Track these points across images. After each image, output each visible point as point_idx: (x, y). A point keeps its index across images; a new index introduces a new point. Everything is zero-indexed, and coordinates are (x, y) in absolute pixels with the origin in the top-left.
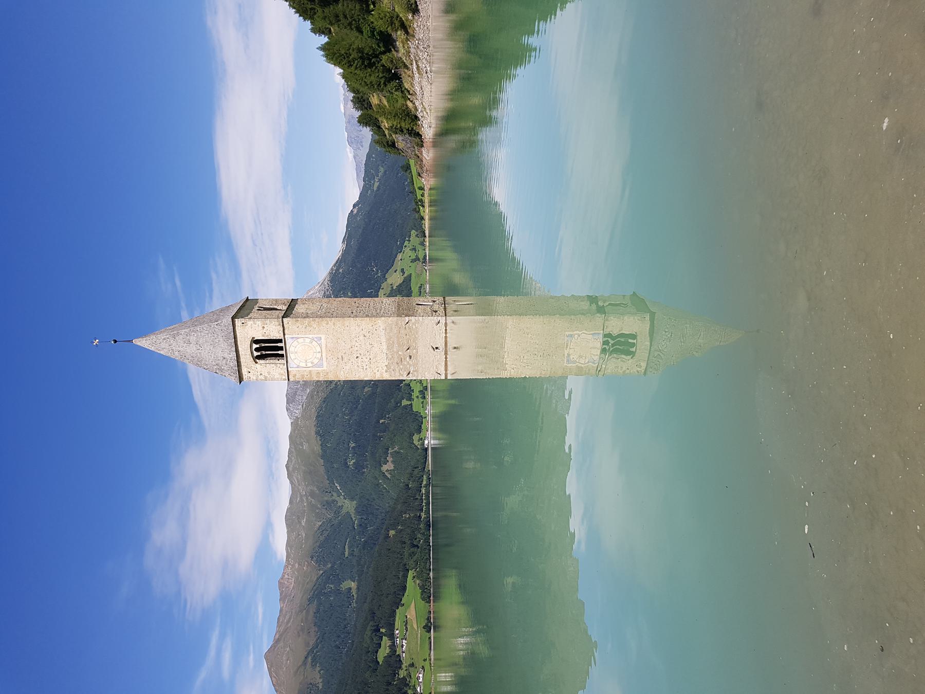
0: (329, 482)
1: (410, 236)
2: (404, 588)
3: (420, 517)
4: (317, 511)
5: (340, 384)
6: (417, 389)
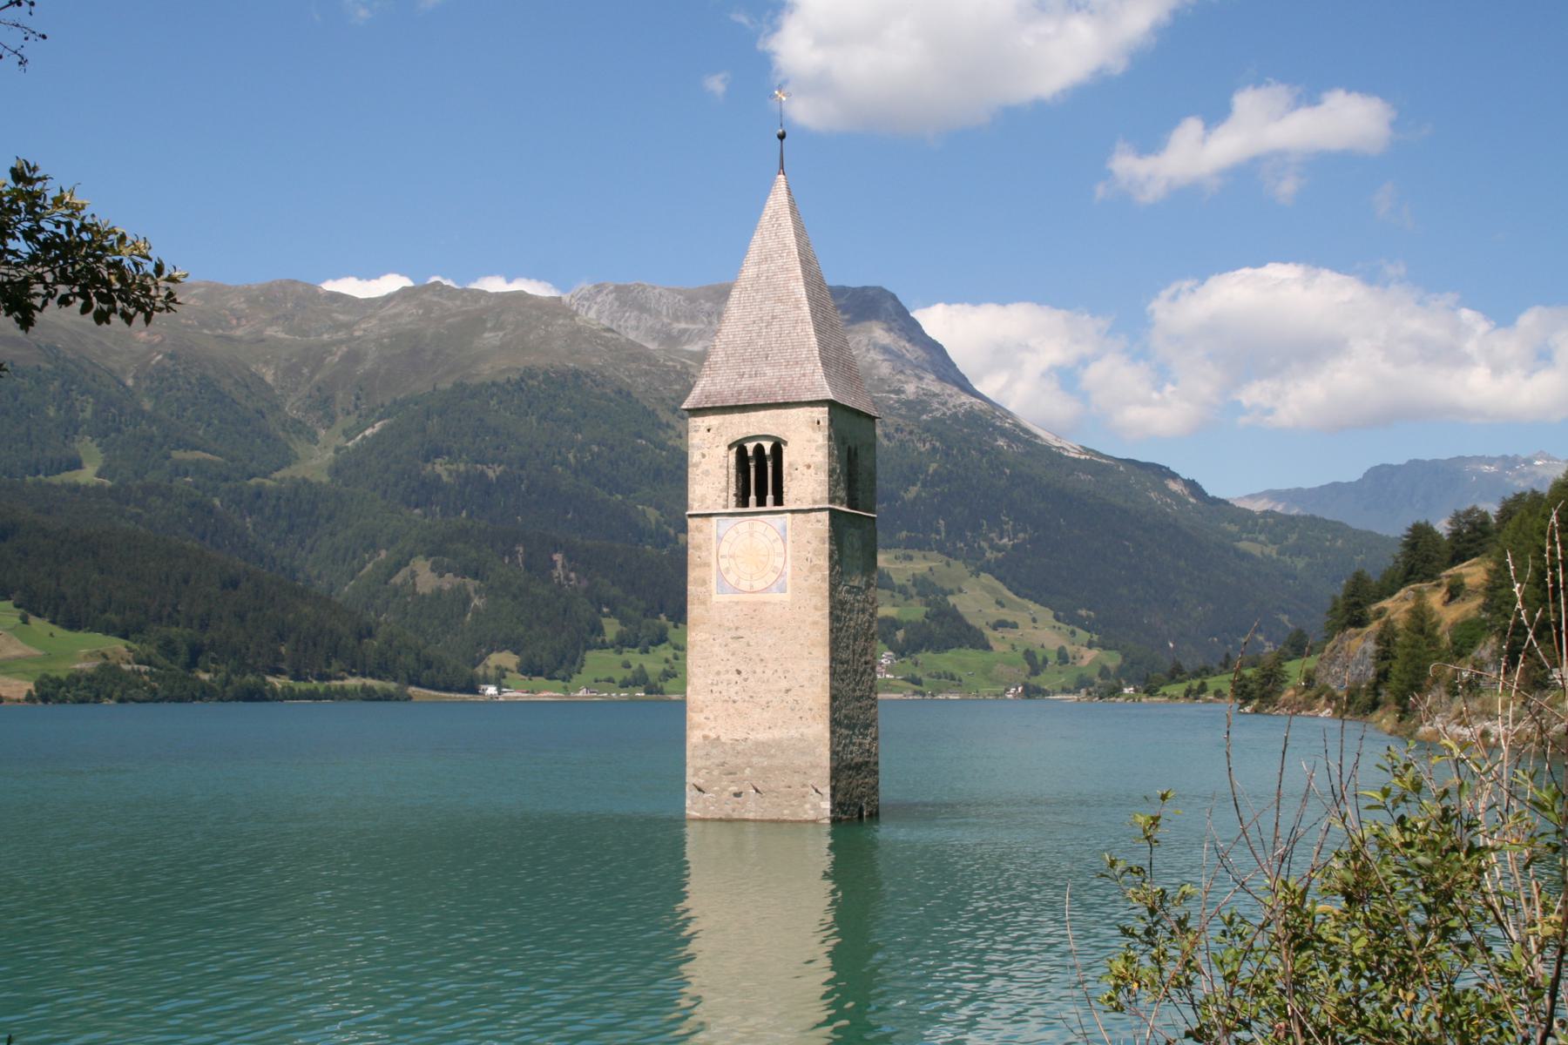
0: (387, 403)
1: (1104, 647)
2: (73, 624)
3: (276, 672)
4: (305, 371)
5: (670, 438)
6: (652, 663)
